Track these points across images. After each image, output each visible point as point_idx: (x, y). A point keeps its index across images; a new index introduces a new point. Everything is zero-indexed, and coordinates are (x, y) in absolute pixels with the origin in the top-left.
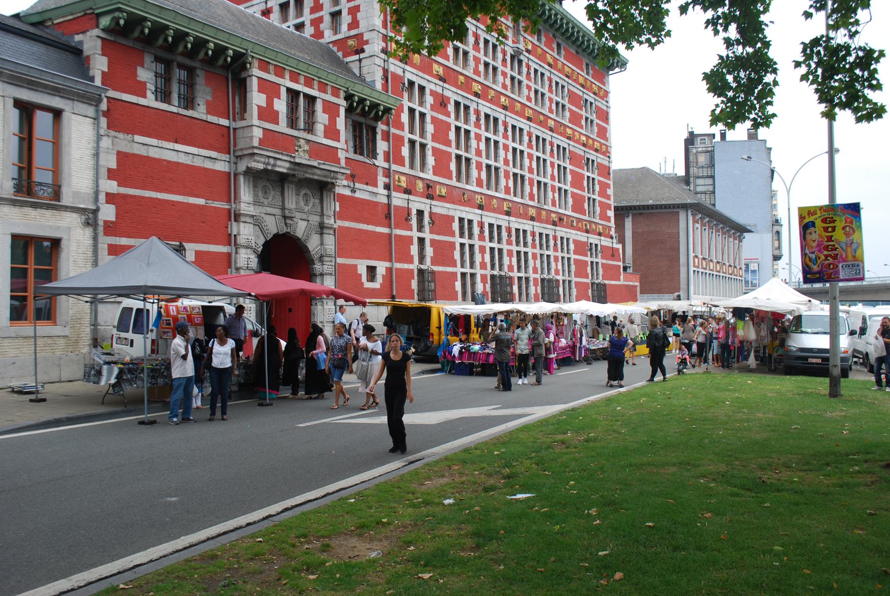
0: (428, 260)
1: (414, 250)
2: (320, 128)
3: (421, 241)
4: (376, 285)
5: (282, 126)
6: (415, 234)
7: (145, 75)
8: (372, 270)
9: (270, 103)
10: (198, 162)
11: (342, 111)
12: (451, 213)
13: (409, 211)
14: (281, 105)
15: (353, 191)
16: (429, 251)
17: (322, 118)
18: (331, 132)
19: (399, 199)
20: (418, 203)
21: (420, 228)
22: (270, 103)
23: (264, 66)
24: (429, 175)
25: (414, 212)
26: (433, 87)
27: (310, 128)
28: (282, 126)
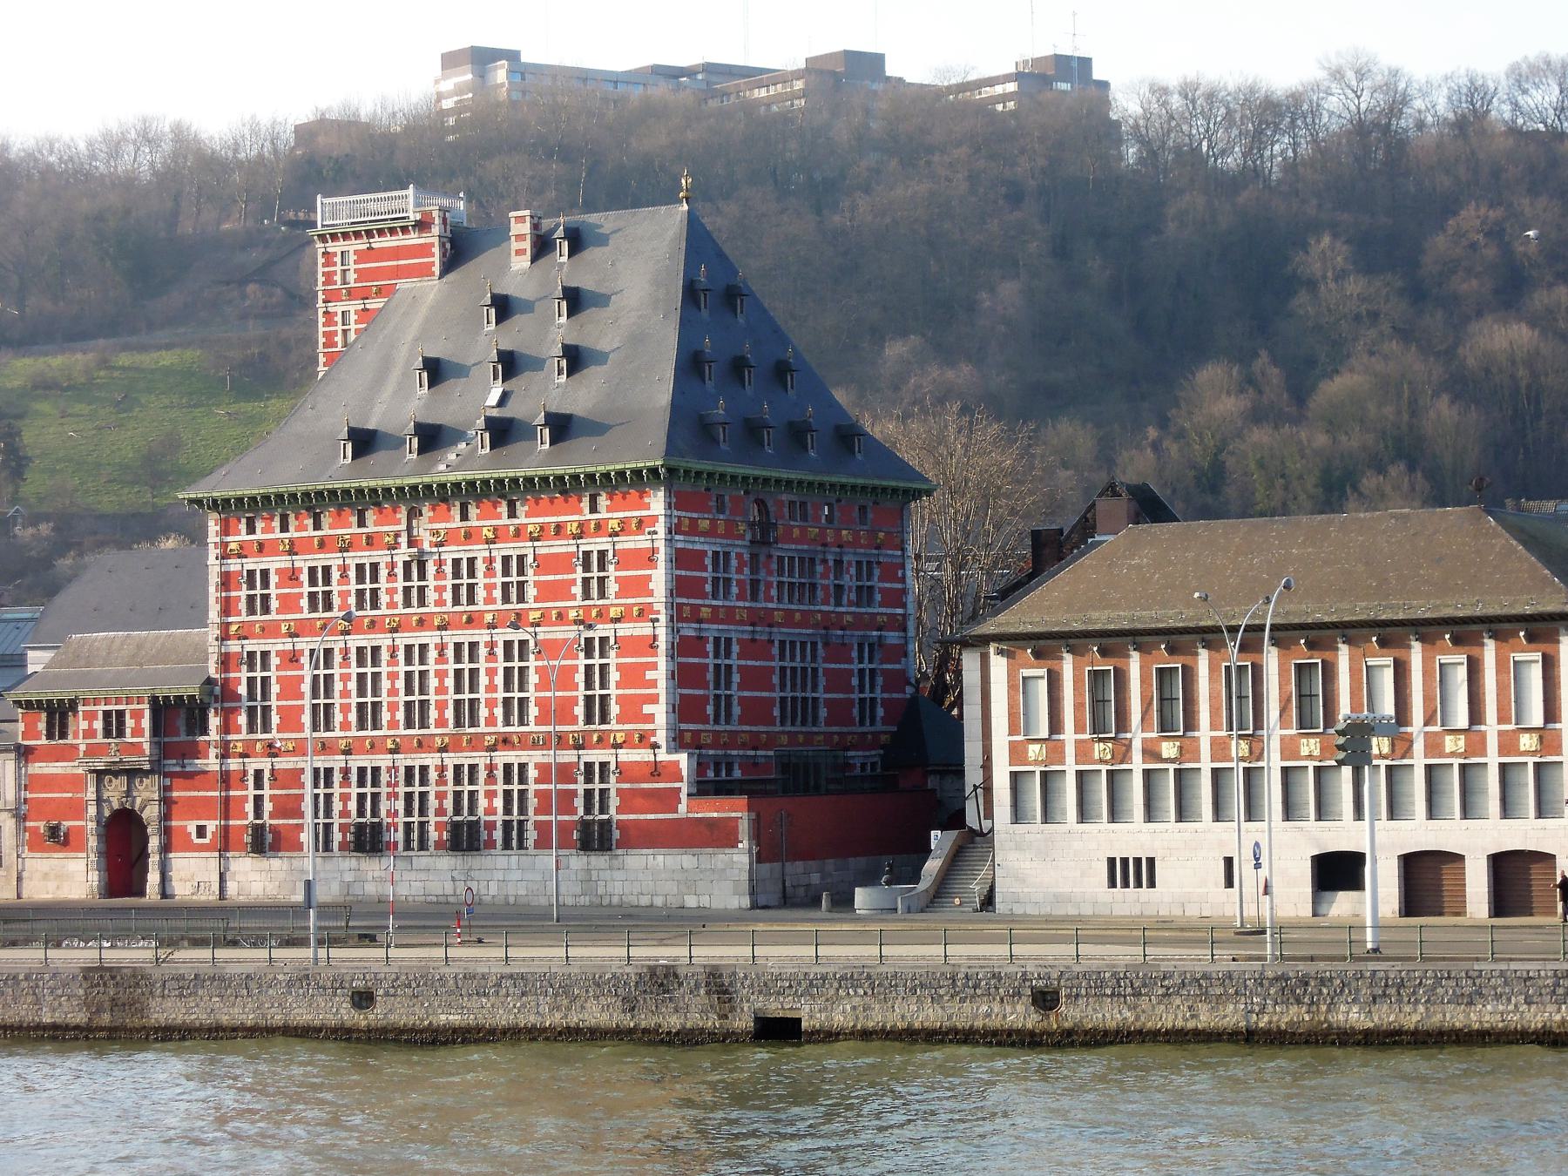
0: (266, 815)
1: (249, 807)
2: (128, 731)
3: (258, 800)
4: (206, 841)
5: (100, 739)
6: (251, 792)
7: (42, 726)
8: (201, 831)
9: (90, 725)
10: (69, 771)
11: (147, 713)
12: (301, 765)
13: (245, 773)
14: (98, 725)
15: (183, 766)
16: (268, 806)
17: (130, 723)
18: (137, 732)
19: (234, 764)
20: (253, 765)
21: (258, 784)
22: (90, 725)
23: (86, 702)
24: (274, 734)
25: (251, 772)
26: (280, 647)
27: (121, 733)
28: (100, 739)
